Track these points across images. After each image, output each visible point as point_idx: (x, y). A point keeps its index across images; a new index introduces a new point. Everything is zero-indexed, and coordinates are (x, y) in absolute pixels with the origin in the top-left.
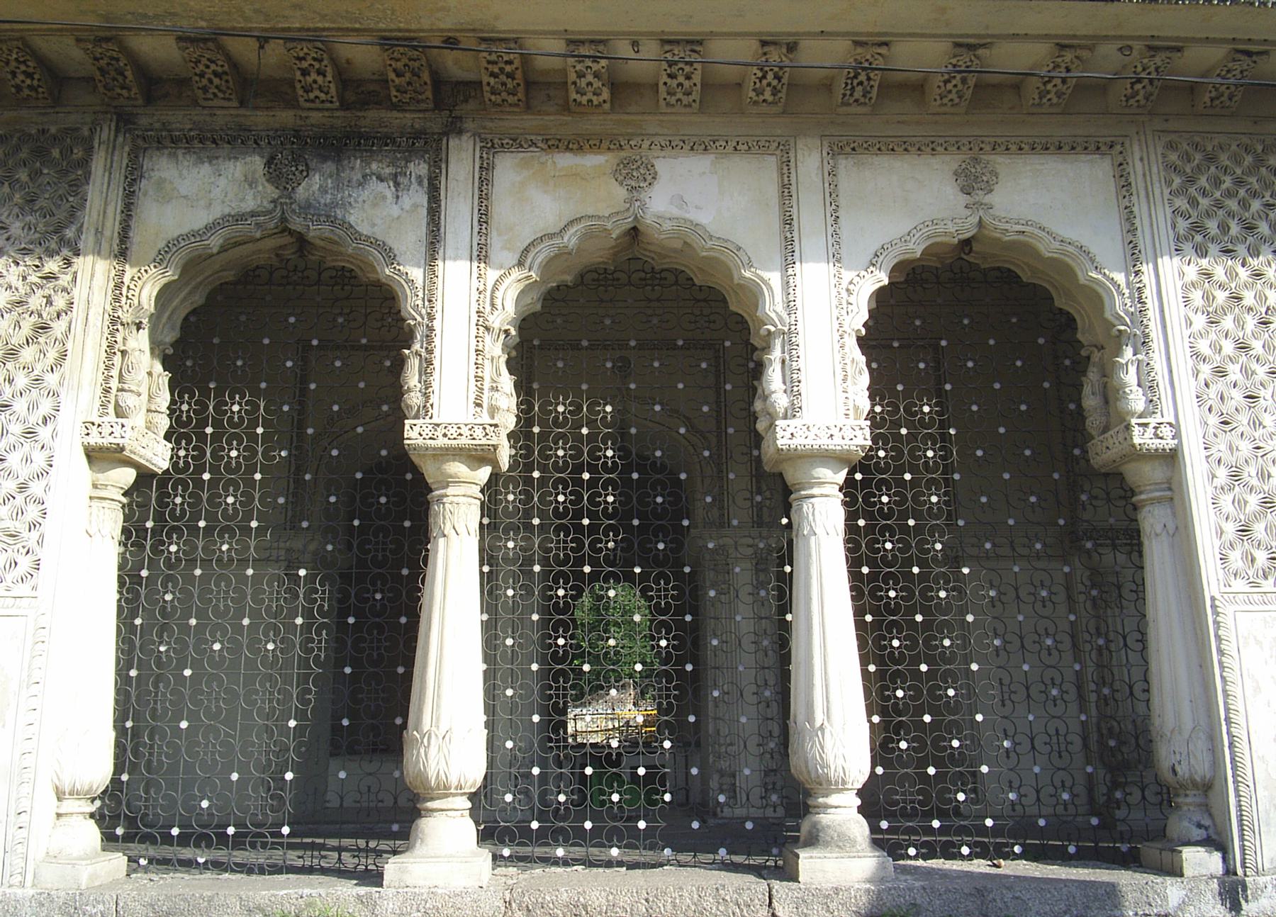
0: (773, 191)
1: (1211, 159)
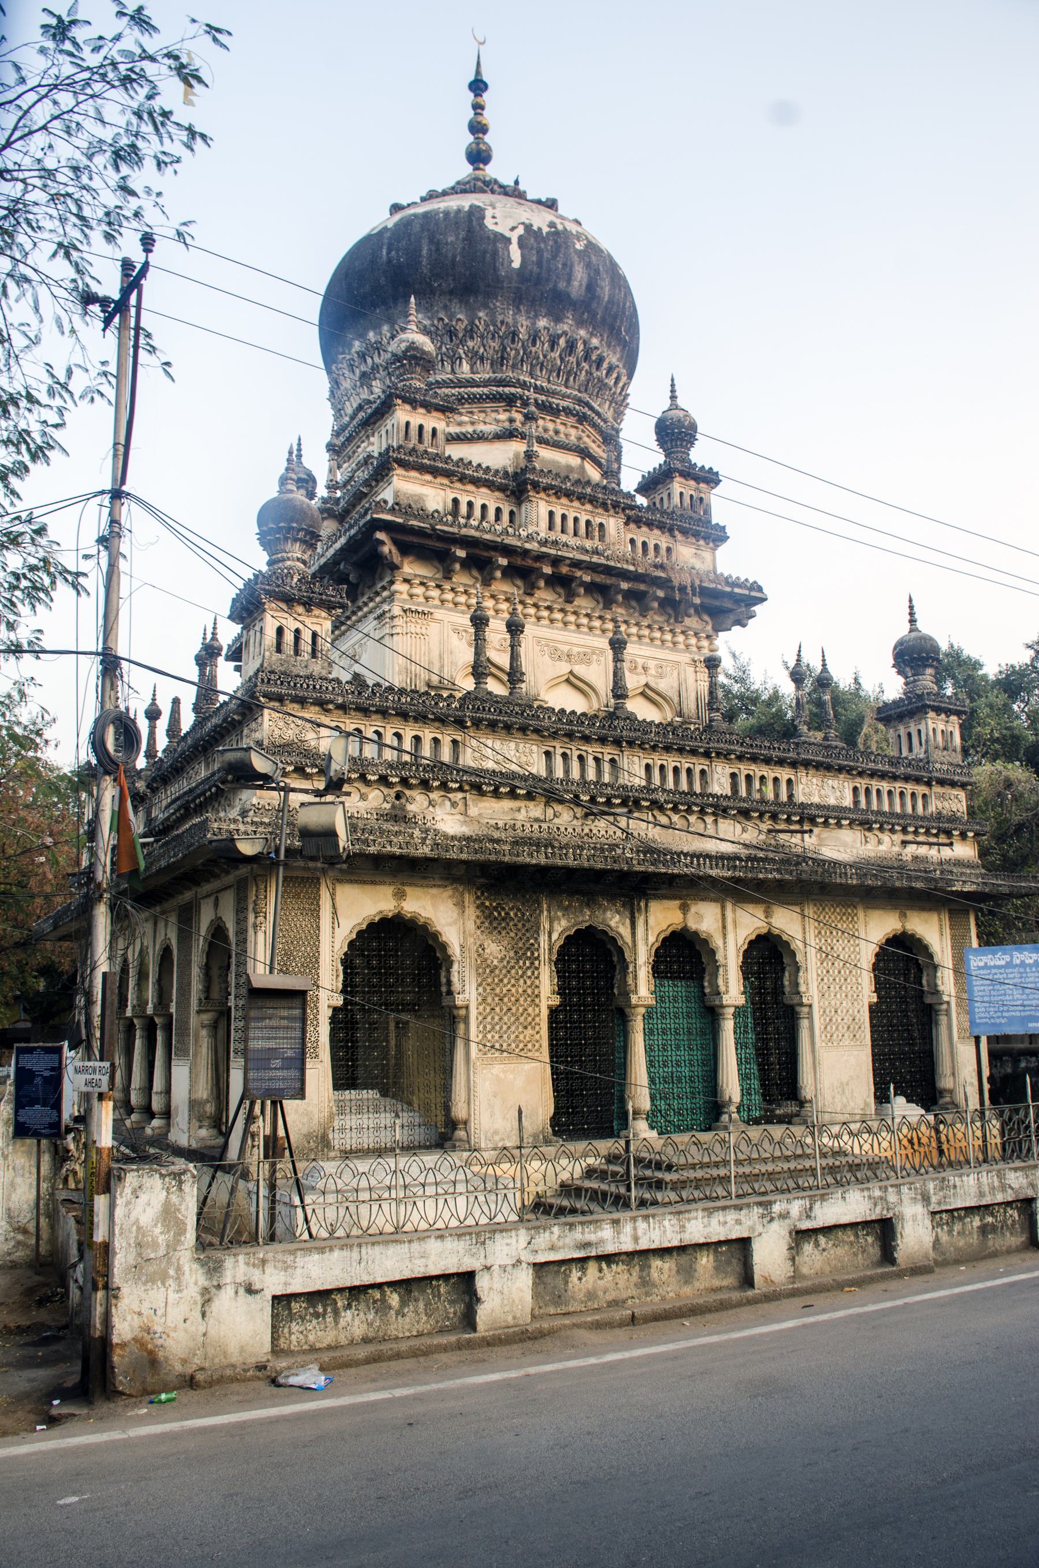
0: (719, 916)
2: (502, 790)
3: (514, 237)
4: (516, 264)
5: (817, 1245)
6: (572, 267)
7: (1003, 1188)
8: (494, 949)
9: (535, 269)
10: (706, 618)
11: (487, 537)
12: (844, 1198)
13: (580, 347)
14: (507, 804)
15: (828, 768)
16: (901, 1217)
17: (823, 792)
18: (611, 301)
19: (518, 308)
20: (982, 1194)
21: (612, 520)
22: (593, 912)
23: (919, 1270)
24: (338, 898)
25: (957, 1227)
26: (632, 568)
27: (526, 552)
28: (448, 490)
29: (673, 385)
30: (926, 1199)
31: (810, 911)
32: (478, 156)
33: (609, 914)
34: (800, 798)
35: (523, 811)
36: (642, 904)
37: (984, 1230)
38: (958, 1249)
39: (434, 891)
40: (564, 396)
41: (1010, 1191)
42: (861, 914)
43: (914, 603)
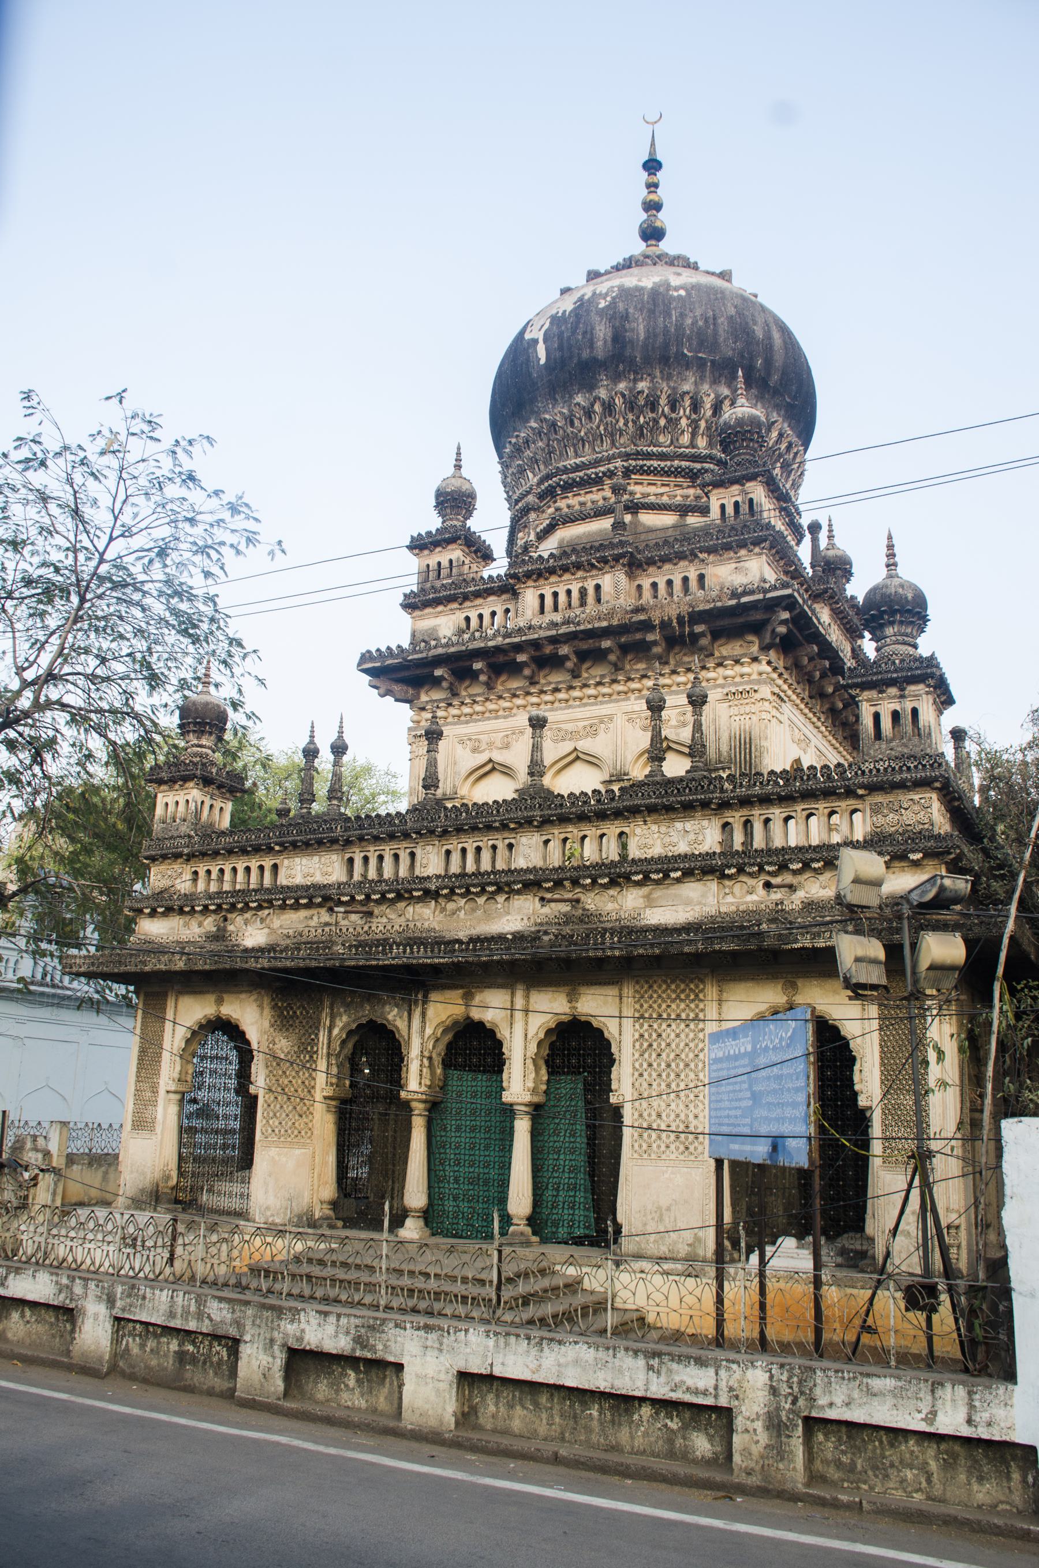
1: (651, 987)
2: (589, 881)
3: (540, 336)
4: (543, 361)
5: (23, 1316)
6: (593, 329)
7: (200, 1316)
8: (284, 1045)
10: (751, 638)
11: (452, 650)
12: (34, 1276)
14: (303, 913)
15: (669, 809)
16: (82, 1312)
17: (667, 840)
18: (651, 335)
19: (556, 400)
20: (172, 1315)
22: (372, 1007)
23: (87, 1370)
24: (179, 1007)
25: (151, 1344)
26: (605, 624)
27: (498, 649)
28: (458, 613)
29: (459, 454)
30: (111, 1301)
31: (628, 990)
32: (652, 234)
33: (387, 1008)
34: (634, 852)
35: (315, 918)
36: (420, 996)
37: (181, 1357)
38: (147, 1367)
39: (243, 996)
40: (610, 459)
41: (207, 1321)
42: (711, 991)
43: (895, 542)
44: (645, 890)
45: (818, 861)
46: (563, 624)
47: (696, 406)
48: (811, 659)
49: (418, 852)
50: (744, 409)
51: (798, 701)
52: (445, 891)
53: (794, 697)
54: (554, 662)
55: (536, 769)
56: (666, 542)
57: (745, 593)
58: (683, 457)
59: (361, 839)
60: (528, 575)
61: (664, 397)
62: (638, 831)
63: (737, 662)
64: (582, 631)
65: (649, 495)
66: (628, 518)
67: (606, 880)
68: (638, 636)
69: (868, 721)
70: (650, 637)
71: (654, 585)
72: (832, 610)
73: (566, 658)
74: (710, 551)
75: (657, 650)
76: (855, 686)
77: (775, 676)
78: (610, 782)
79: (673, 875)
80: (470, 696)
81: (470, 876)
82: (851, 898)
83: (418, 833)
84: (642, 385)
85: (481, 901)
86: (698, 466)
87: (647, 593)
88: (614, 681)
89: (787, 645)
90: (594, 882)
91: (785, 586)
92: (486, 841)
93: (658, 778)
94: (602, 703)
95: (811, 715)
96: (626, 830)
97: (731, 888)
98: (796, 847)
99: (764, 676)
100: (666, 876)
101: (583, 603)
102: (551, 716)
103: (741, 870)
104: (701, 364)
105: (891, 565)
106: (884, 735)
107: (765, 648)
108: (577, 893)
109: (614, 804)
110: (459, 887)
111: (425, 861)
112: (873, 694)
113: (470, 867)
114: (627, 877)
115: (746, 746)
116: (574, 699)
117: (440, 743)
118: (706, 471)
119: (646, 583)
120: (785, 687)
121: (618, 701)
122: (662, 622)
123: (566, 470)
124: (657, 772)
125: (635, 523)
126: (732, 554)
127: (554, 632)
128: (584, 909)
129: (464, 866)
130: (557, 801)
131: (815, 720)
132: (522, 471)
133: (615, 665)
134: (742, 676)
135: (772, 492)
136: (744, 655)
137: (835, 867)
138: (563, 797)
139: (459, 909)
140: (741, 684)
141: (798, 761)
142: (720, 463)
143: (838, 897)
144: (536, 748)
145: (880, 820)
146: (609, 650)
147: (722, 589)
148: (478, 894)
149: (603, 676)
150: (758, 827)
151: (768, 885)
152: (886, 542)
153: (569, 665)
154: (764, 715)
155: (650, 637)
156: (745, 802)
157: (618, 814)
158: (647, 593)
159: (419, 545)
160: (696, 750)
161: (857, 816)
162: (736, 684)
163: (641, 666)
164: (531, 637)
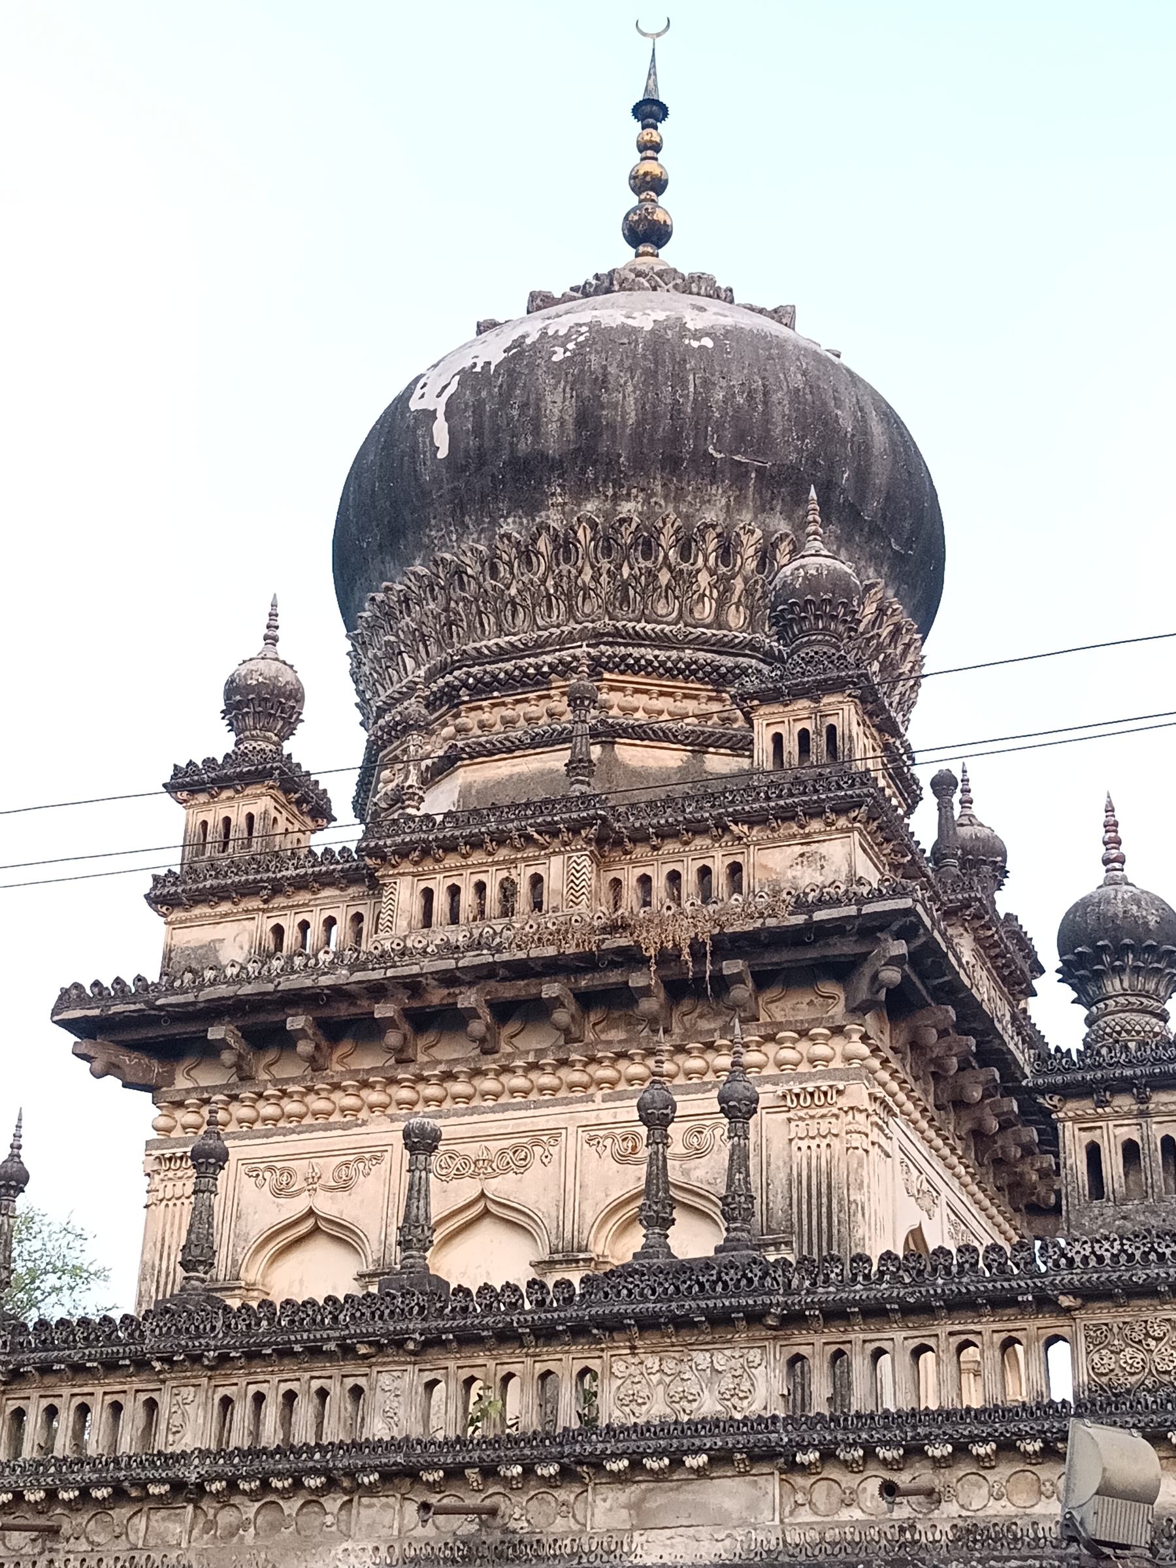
4: (442, 454)
9: (472, 443)
10: (829, 988)
11: (248, 989)
13: (583, 534)
15: (682, 1323)
21: (556, 862)
26: (551, 951)
27: (338, 993)
28: (260, 918)
32: (647, 233)
34: (610, 1412)
44: (632, 1492)
45: (985, 1441)
46: (469, 948)
47: (727, 551)
48: (943, 1033)
49: (165, 1401)
50: (819, 559)
51: (916, 1115)
52: (217, 1486)
53: (909, 1106)
54: (449, 1021)
55: (415, 1233)
56: (669, 800)
57: (821, 903)
58: (701, 643)
59: (45, 1369)
60: (403, 852)
61: (668, 530)
62: (619, 1367)
63: (803, 1034)
64: (506, 964)
65: (636, 710)
66: (596, 751)
67: (553, 1469)
68: (614, 977)
69: (1077, 1160)
70: (637, 980)
71: (645, 880)
72: (977, 940)
73: (472, 1014)
74: (751, 821)
75: (648, 1005)
76: (1052, 1090)
77: (875, 1063)
78: (550, 1264)
79: (689, 1461)
80: (275, 1082)
81: (272, 1455)
82: (1095, 1528)
83: (167, 1360)
84: (627, 508)
85: (291, 1506)
86: (729, 661)
87: (631, 895)
88: (563, 1063)
89: (897, 1005)
90: (528, 1471)
91: (898, 892)
92: (305, 1381)
93: (660, 1261)
94: (537, 1105)
95: (939, 1142)
96: (595, 1364)
97: (808, 1492)
98: (940, 1411)
99: (856, 1064)
100: (677, 1463)
101: (507, 911)
102: (449, 1128)
103: (828, 1455)
104: (739, 474)
105: (1113, 861)
106: (1108, 1189)
107: (857, 1010)
108: (492, 1495)
109: (571, 1312)
110: (248, 1478)
111: (177, 1420)
112: (1085, 1106)
113: (271, 1436)
114: (596, 1464)
115: (824, 1201)
116: (484, 1095)
117: (222, 1175)
118: (744, 672)
119: (630, 876)
120: (894, 1086)
121: (568, 1102)
122: (662, 951)
123: (479, 658)
124: (656, 1247)
125: (612, 763)
126: (795, 829)
127: (451, 964)
128: (506, 1530)
129: (256, 1435)
130: (458, 1302)
131: (946, 1151)
132: (393, 654)
133: (566, 1031)
134: (812, 1061)
135: (871, 715)
136: (817, 1022)
137: (1061, 1457)
138: (468, 1292)
139: (244, 1525)
140: (811, 1077)
141: (917, 1234)
142: (769, 657)
143: (1070, 1529)
144: (417, 1192)
145: (1108, 1361)
146: (556, 1002)
147: (776, 893)
148: (284, 1493)
149: (541, 1053)
150: (859, 1364)
151: (889, 1490)
152: (1102, 817)
153: (477, 1027)
154: (856, 1140)
155: (637, 980)
156: (835, 1315)
157: (579, 1331)
158: (631, 895)
159: (188, 783)
160: (735, 1205)
161: (1060, 1351)
162: (802, 1077)
163: (617, 1035)
164: (406, 971)
